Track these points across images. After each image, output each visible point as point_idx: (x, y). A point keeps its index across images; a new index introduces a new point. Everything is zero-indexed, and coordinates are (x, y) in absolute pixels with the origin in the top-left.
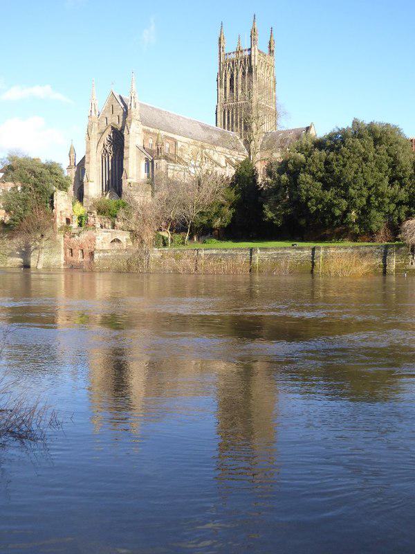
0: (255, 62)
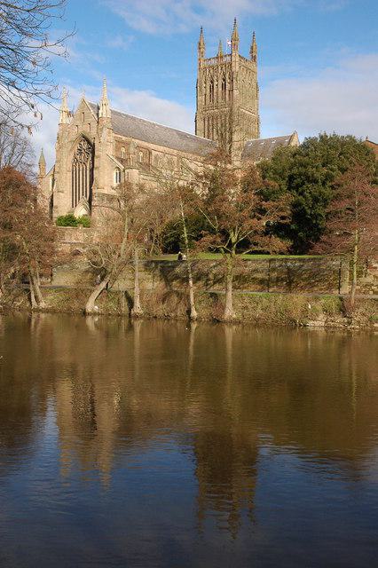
0: (236, 68)
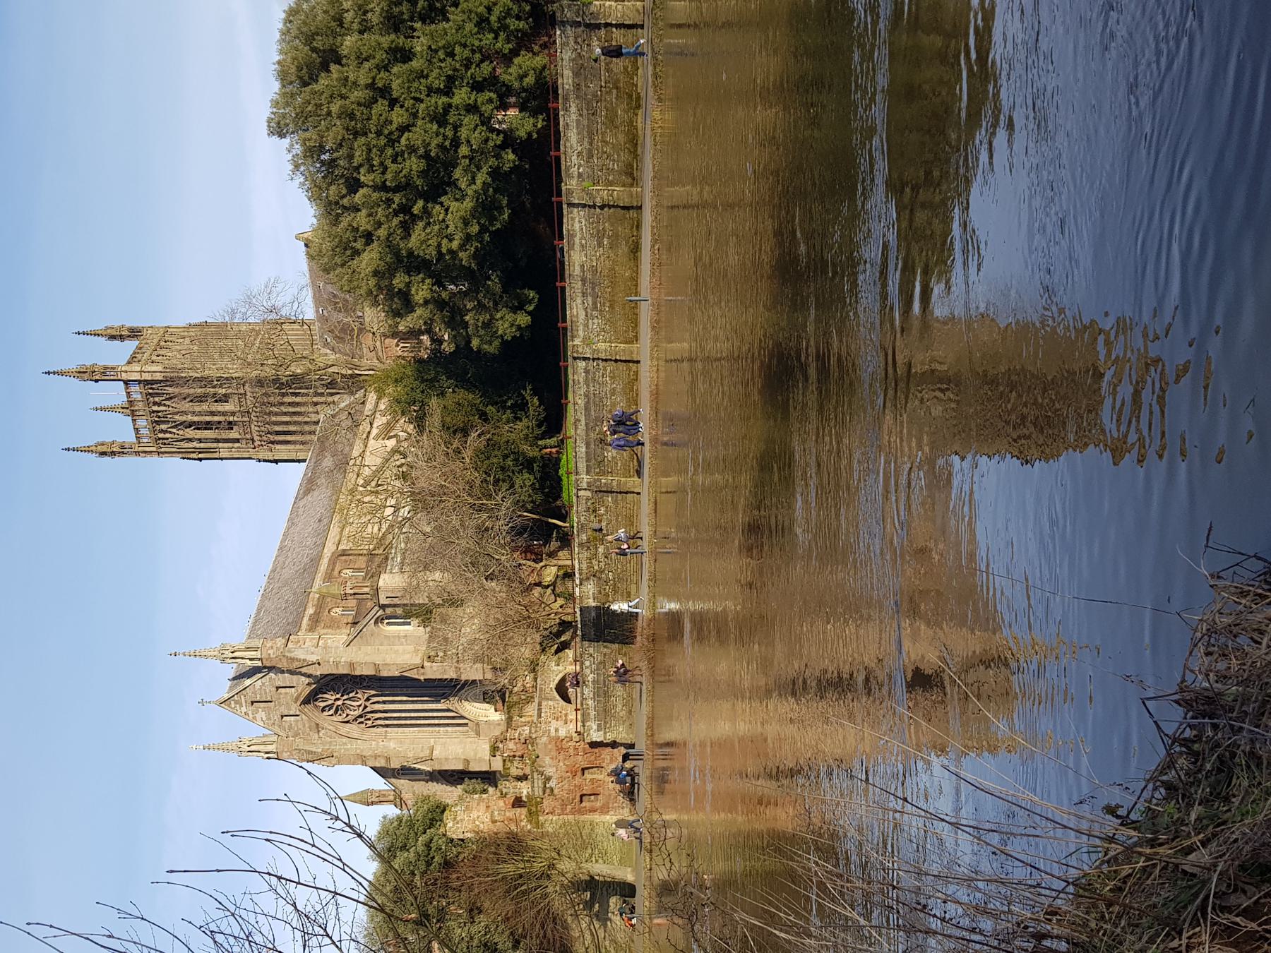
0: (155, 371)
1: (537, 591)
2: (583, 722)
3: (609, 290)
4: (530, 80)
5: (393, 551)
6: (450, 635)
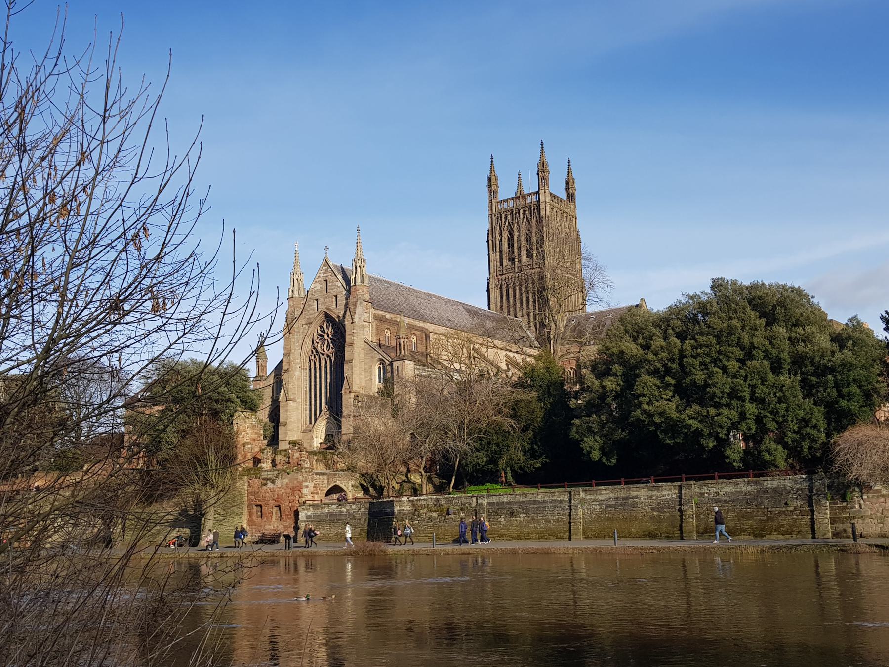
0: (546, 210)
1: (403, 469)
2: (312, 505)
3: (621, 517)
4: (767, 457)
5: (429, 369)
6: (372, 410)
